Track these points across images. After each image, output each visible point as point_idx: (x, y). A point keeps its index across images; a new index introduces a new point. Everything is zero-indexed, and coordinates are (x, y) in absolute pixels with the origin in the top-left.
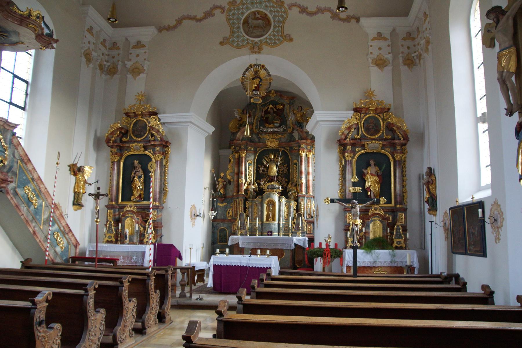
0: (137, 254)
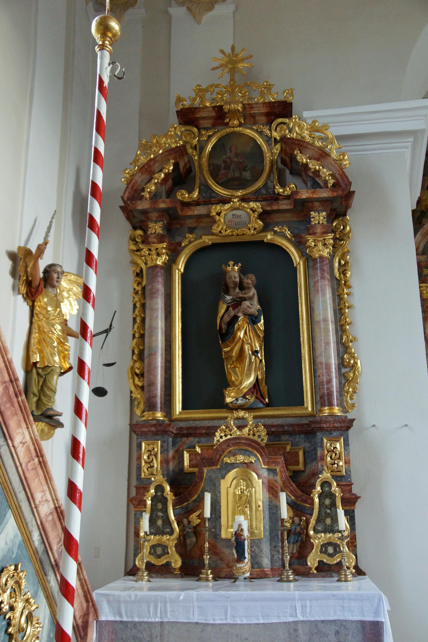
0: (337, 633)
